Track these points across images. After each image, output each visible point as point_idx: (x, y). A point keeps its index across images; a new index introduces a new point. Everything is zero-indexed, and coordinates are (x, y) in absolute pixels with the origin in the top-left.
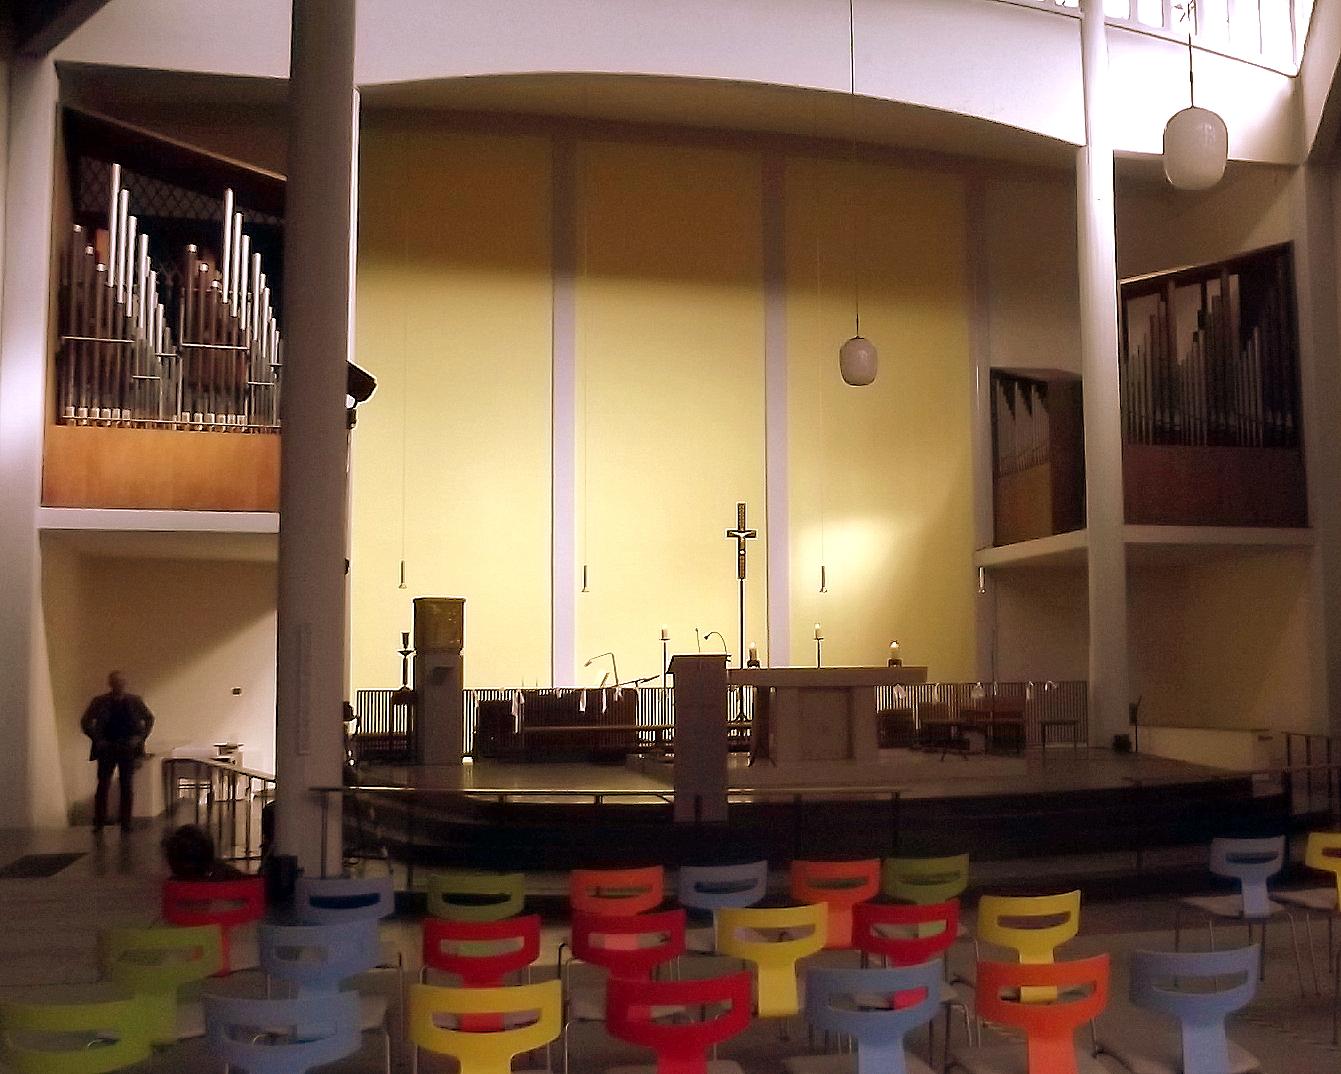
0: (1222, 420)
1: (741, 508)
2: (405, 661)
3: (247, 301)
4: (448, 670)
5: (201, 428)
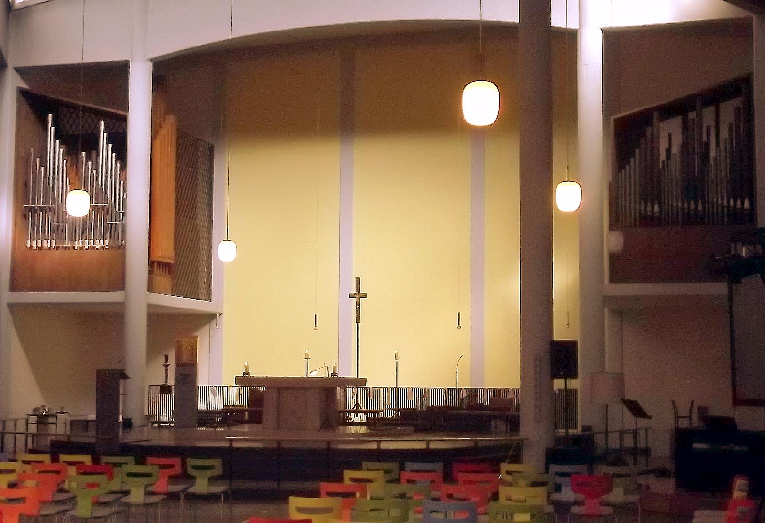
1: (358, 280)
4: (189, 375)
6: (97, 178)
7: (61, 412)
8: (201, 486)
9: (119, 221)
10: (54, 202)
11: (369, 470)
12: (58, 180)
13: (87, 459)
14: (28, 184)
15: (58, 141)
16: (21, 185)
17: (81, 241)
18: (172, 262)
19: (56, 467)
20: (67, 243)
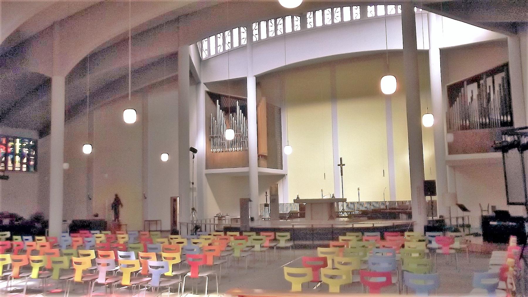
0: (484, 120)
1: (341, 159)
5: (234, 151)
7: (227, 215)
8: (282, 243)
11: (349, 236)
13: (237, 234)
17: (231, 148)
18: (267, 155)
19: (226, 237)
20: (226, 149)
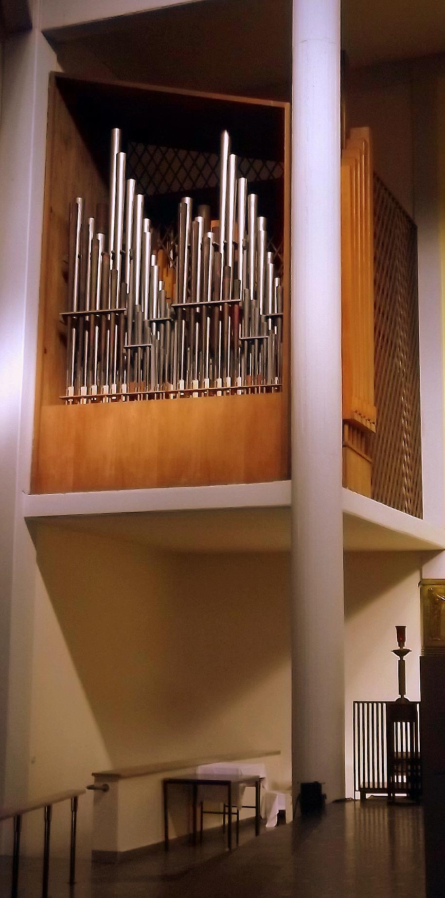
2: (402, 666)
3: (244, 249)
6: (216, 248)
9: (268, 334)
10: (124, 297)
12: (133, 258)
14: (71, 273)
15: (132, 182)
16: (56, 276)
17: (182, 382)
